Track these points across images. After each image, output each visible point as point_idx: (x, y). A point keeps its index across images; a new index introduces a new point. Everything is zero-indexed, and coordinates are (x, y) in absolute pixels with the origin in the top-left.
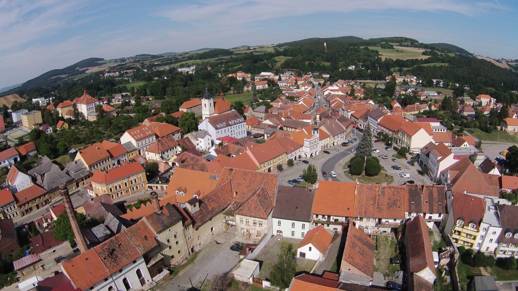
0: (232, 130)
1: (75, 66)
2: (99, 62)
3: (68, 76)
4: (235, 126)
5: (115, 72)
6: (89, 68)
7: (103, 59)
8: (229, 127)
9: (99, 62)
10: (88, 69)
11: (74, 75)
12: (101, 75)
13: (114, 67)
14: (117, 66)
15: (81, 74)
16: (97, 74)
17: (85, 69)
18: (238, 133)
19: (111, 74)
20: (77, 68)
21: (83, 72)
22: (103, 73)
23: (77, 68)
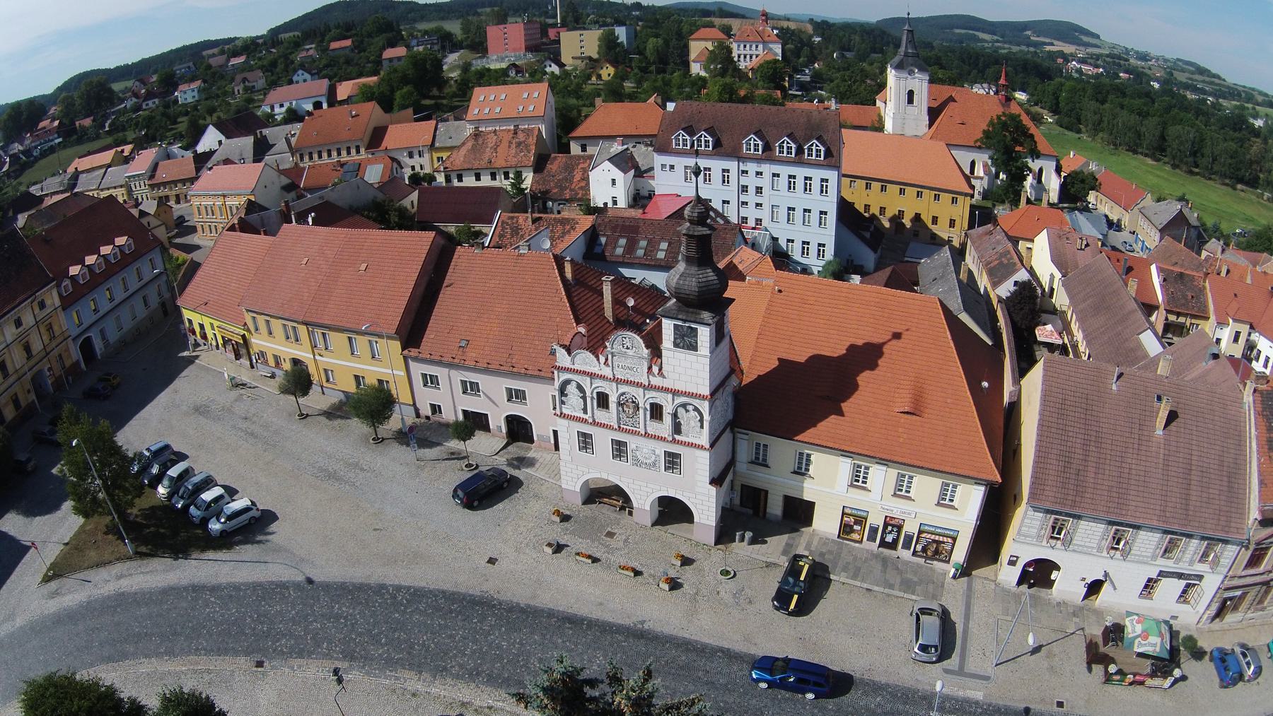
0: (751, 181)
1: (1025, 26)
2: (1085, 39)
3: (998, 41)
4: (768, 169)
5: (1097, 67)
6: (1055, 42)
7: (1098, 37)
8: (732, 165)
9: (1085, 39)
10: (1052, 44)
11: (1010, 43)
12: (1060, 61)
13: (1098, 57)
14: (1107, 56)
15: (1028, 45)
16: (1052, 56)
17: (1047, 40)
18: (783, 213)
19: (1085, 68)
20: (1029, 33)
21: (1036, 45)
22: (1067, 58)
23: (1029, 33)
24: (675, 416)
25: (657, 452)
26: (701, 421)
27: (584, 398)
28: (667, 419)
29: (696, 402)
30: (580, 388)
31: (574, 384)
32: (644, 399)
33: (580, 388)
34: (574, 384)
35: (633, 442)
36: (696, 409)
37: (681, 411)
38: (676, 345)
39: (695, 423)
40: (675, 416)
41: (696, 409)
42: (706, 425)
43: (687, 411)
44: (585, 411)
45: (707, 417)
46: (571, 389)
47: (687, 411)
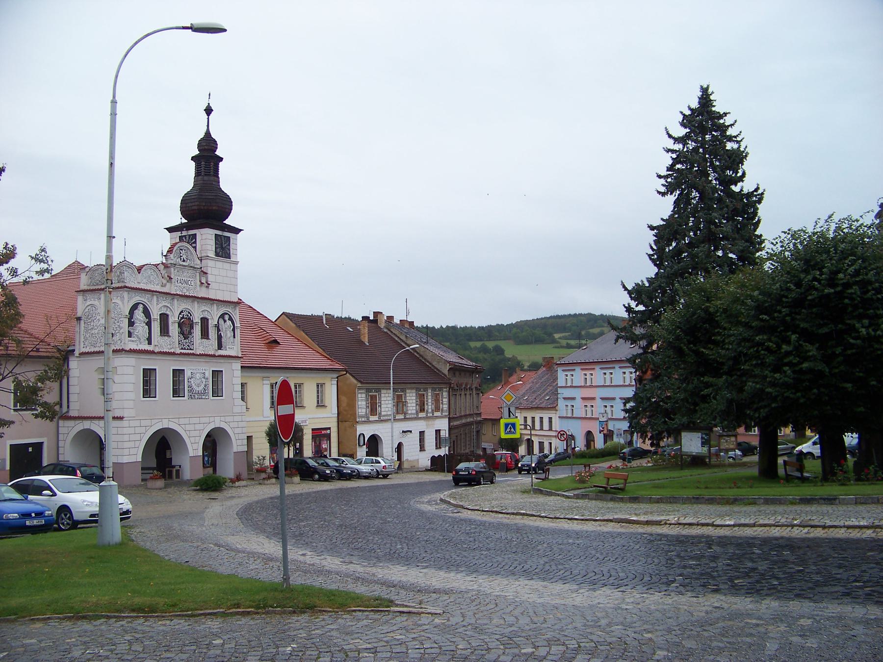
24: (217, 327)
25: (207, 375)
26: (234, 330)
27: (149, 324)
28: (212, 333)
29: (229, 309)
30: (147, 312)
31: (141, 307)
32: (197, 313)
33: (147, 312)
34: (141, 307)
35: (190, 368)
36: (230, 319)
37: (221, 321)
38: (217, 254)
39: (230, 334)
40: (217, 327)
41: (230, 319)
42: (238, 332)
43: (225, 321)
44: (150, 343)
45: (237, 324)
46: (139, 314)
47: (225, 321)
